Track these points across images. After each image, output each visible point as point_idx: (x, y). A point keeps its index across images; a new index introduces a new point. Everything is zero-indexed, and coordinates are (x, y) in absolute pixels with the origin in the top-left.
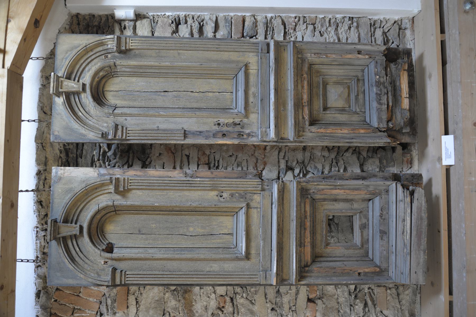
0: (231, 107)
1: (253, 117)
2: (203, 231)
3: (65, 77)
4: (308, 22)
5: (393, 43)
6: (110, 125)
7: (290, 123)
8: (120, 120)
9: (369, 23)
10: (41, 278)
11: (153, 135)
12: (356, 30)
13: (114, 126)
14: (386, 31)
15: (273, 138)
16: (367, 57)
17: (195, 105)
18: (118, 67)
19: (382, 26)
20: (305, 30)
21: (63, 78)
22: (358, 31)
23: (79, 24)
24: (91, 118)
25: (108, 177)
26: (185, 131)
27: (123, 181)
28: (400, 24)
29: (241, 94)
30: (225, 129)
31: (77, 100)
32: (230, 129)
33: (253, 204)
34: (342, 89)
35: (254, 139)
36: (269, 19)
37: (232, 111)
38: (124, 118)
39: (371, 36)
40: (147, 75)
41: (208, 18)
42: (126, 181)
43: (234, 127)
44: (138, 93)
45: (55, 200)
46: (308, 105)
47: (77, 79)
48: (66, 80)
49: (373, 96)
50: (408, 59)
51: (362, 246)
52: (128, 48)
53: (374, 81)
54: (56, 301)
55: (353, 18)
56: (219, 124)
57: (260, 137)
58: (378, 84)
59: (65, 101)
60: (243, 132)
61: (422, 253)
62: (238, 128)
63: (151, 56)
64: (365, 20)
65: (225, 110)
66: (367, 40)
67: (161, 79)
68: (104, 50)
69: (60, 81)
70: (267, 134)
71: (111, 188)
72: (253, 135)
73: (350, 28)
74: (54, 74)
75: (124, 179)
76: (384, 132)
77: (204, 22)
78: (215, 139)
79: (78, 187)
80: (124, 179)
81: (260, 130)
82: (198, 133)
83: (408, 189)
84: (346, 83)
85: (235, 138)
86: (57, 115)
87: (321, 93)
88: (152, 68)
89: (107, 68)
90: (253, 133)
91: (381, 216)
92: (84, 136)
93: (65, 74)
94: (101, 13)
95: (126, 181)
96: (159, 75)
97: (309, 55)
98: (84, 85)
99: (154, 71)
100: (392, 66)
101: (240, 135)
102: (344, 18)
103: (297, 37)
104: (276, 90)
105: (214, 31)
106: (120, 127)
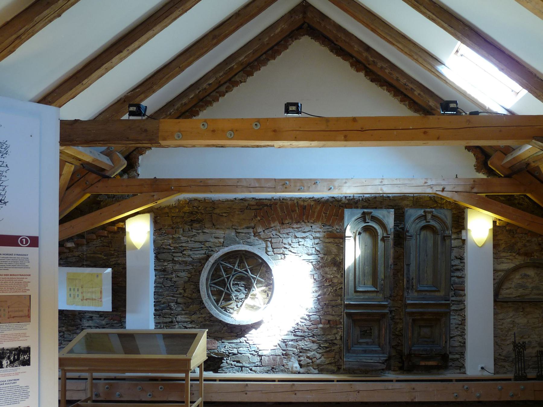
1: (416, 294)
8: (414, 238)
10: (341, 199)
23: (459, 212)
29: (426, 289)
30: (411, 282)
33: (378, 294)
35: (406, 294)
51: (359, 343)
54: (330, 205)
56: (412, 279)
61: (357, 367)
62: (411, 287)
65: (419, 281)
79: (385, 221)
83: (385, 362)
91: (373, 350)
94: (465, 223)
98: (429, 222)
101: (408, 288)
104: (428, 303)
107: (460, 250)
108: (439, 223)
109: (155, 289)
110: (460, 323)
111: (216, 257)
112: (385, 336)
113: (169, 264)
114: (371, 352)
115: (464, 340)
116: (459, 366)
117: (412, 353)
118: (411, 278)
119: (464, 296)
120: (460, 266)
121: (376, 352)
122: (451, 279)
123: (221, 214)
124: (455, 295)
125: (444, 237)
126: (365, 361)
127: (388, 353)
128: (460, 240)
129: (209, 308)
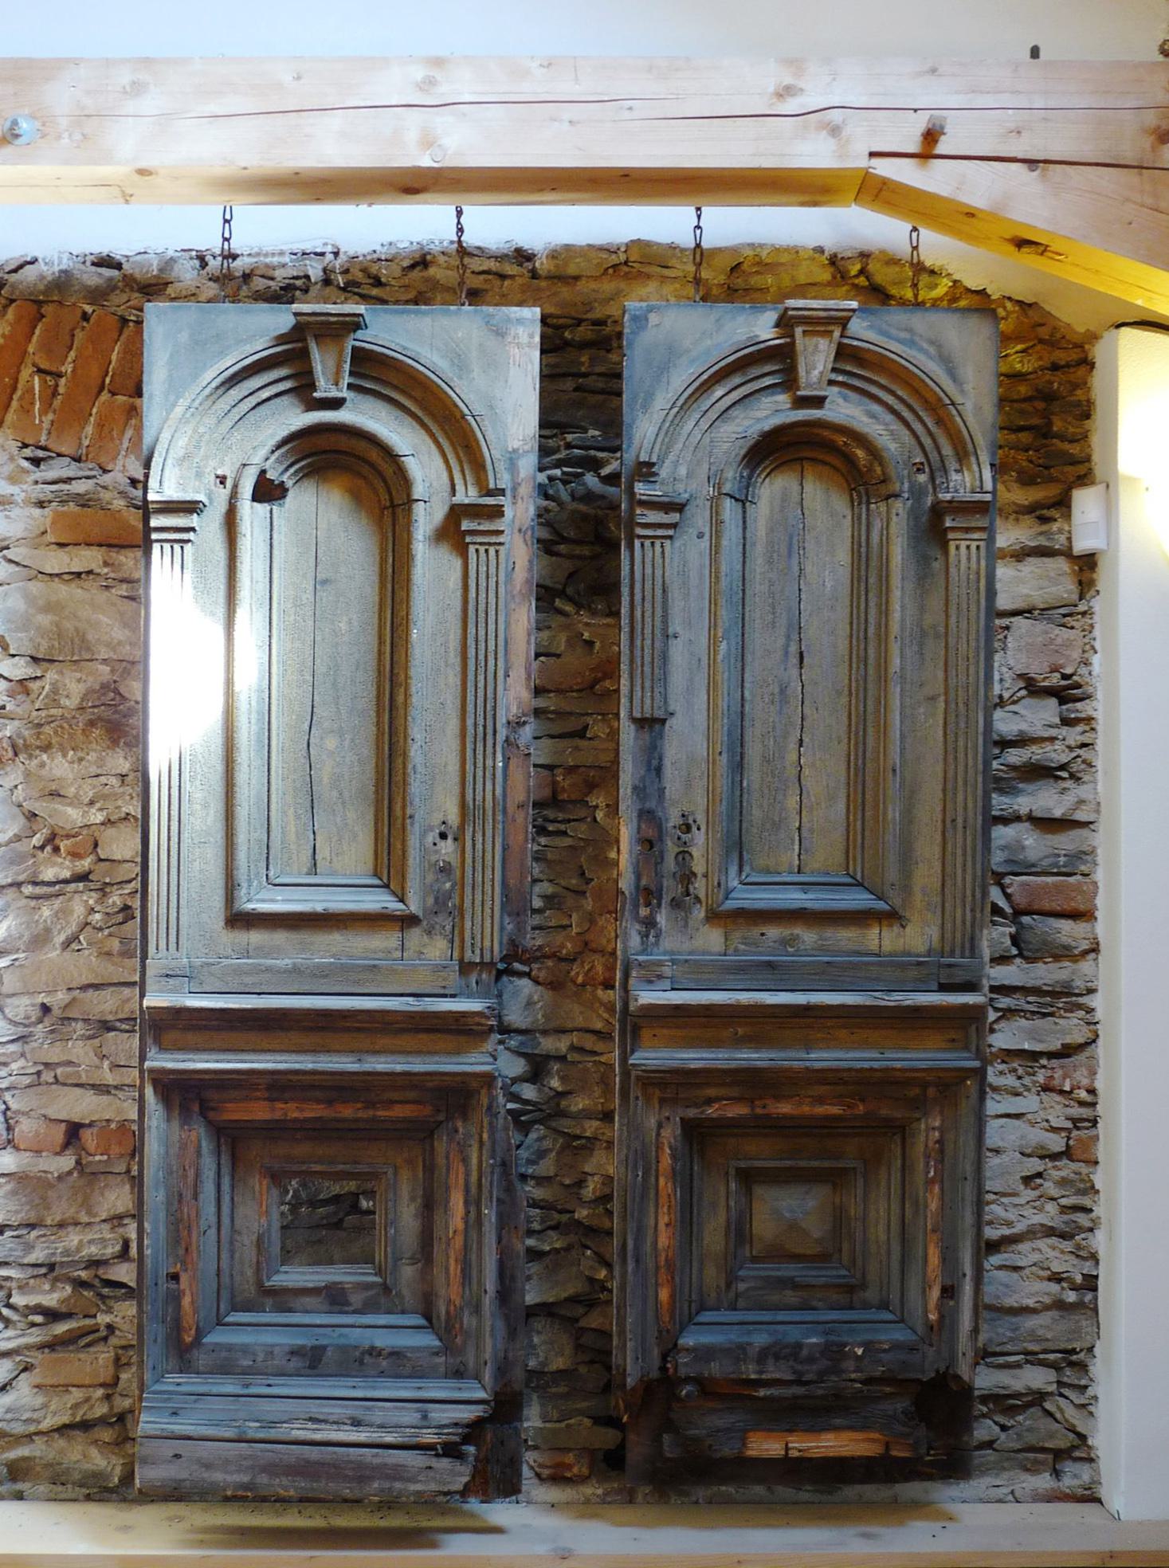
0: (747, 869)
2: (326, 780)
3: (846, 341)
4: (1075, 1133)
5: (1004, 1428)
6: (680, 487)
7: (692, 1056)
8: (699, 518)
9: (1077, 1345)
11: (648, 620)
12: (1047, 1300)
13: (677, 500)
14: (1048, 1405)
15: (636, 1000)
18: (883, 507)
19: (1066, 1391)
20: (1045, 1123)
21: (842, 336)
22: (1047, 1308)
24: (704, 424)
25: (504, 481)
26: (663, 721)
27: (493, 528)
28: (1077, 1454)
29: (794, 898)
31: (768, 381)
32: (670, 864)
34: (816, 1234)
35: (635, 941)
37: (733, 870)
38: (707, 530)
39: (1027, 1353)
40: (859, 598)
41: (1084, 796)
42: (493, 539)
43: (678, 876)
44: (796, 569)
45: (428, 320)
46: (756, 1117)
47: (840, 378)
48: (834, 347)
49: (793, 1334)
50: (931, 1464)
52: (951, 535)
53: (845, 1339)
56: (687, 828)
57: (641, 958)
58: (834, 1352)
59: (762, 346)
60: (659, 905)
63: (922, 609)
64: (1087, 1333)
65: (736, 847)
66: (1012, 1339)
67: (847, 642)
68: (942, 461)
69: (830, 328)
70: (651, 982)
71: (467, 494)
72: (647, 936)
73: (1056, 1278)
74: (854, 310)
75: (500, 532)
76: (663, 1369)
77: (1069, 784)
78: (635, 814)
80: (500, 532)
81: (666, 958)
82: (655, 763)
84: (840, 1251)
85: (638, 877)
86: (717, 321)
87: (803, 1164)
88: (881, 613)
89: (878, 470)
90: (657, 936)
92: (645, 407)
93: (855, 343)
95: (493, 539)
96: (858, 637)
97: (937, 1124)
98: (818, 402)
99: (872, 620)
100: (901, 1405)
101: (649, 895)
103: (1017, 1094)
105: (1034, 814)
106: (674, 517)
110: (1056, 1143)
112: (466, 1247)
115: (1088, 1267)
118: (673, 819)
119: (1086, 953)
121: (397, 1363)
124: (1023, 948)
125: (938, 511)
127: (487, 1375)
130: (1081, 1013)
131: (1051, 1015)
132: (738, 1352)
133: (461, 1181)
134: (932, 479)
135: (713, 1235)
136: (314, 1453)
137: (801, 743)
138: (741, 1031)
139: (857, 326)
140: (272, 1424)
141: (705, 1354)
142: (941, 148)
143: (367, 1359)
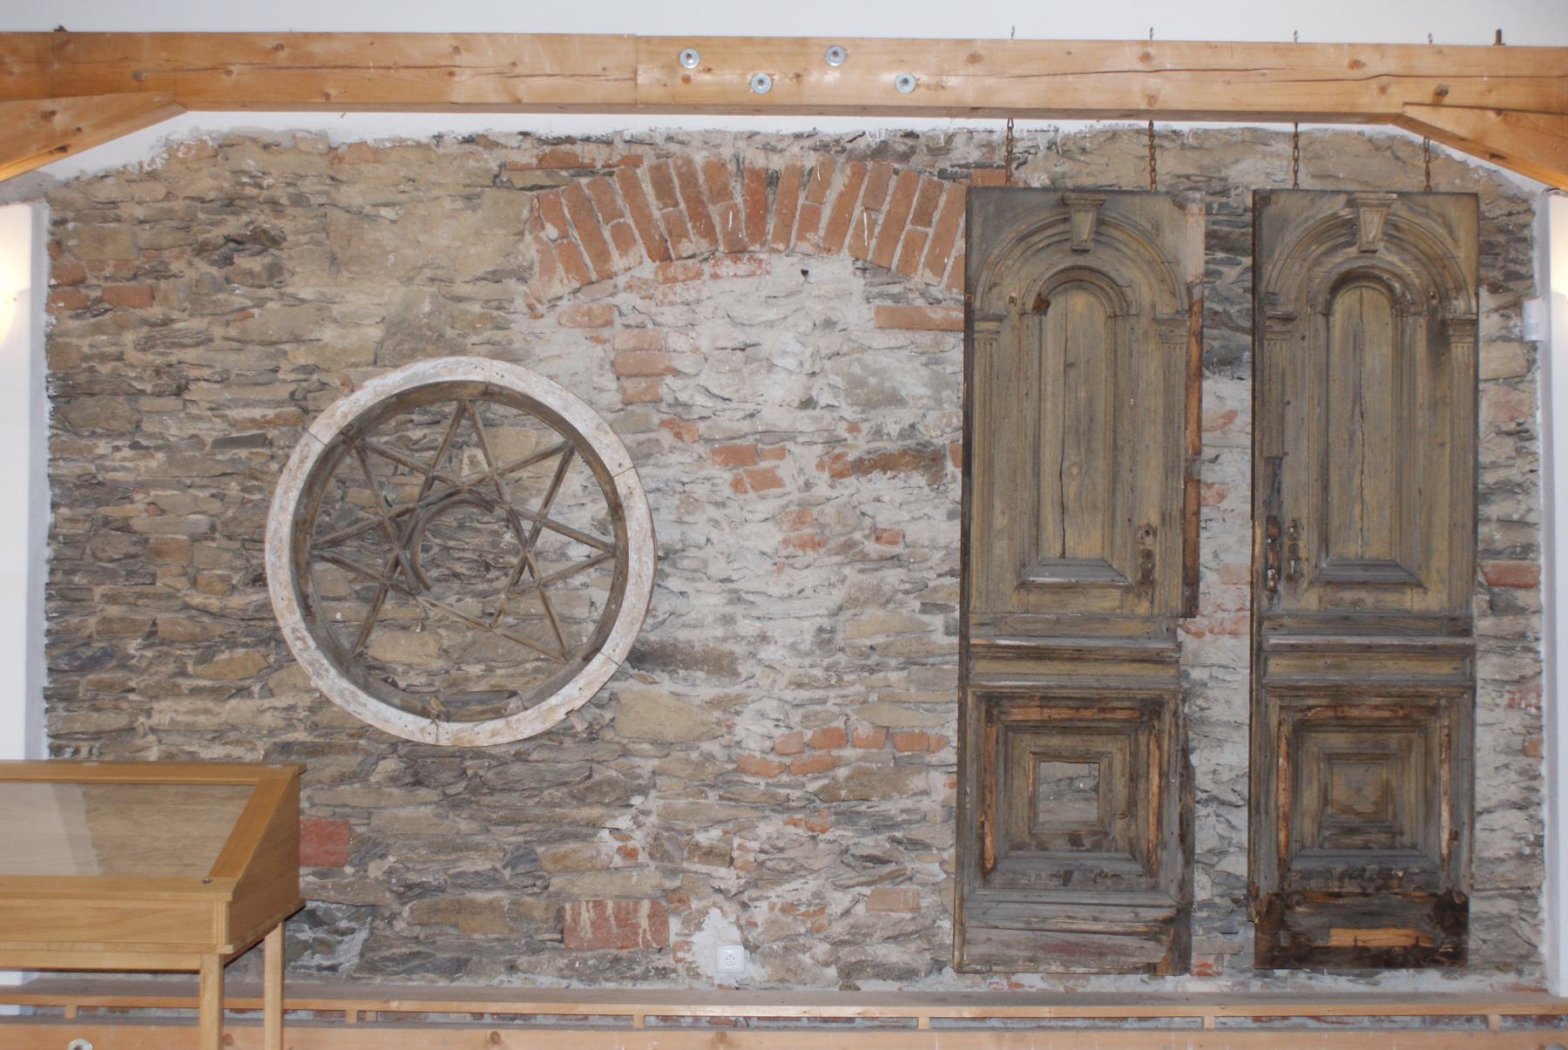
2: (1071, 496)
16: (1445, 851)
17: (1334, 478)
18: (1411, 320)
30: (1287, 542)
31: (1342, 240)
36: (1533, 645)
37: (1323, 554)
50: (1445, 954)
55: (1542, 845)
65: (1325, 541)
89: (1409, 296)
102: (1541, 822)
107: (1515, 396)
108: (1417, 259)
109: (52, 572)
111: (345, 415)
113: (117, 449)
114: (1096, 878)
116: (1514, 952)
117: (1294, 886)
118: (1288, 523)
120: (1514, 471)
122: (1475, 532)
123: (368, 209)
126: (1065, 926)
127: (1173, 889)
128: (1514, 349)
129: (311, 664)
130: (1531, 655)
131: (1512, 655)
132: (1326, 874)
133: (1157, 761)
134: (1441, 302)
135: (1310, 797)
136: (1072, 938)
137: (1362, 473)
138: (1329, 661)
139: (1394, 206)
140: (1044, 919)
141: (1306, 875)
142: (1447, 100)
143: (1099, 879)
